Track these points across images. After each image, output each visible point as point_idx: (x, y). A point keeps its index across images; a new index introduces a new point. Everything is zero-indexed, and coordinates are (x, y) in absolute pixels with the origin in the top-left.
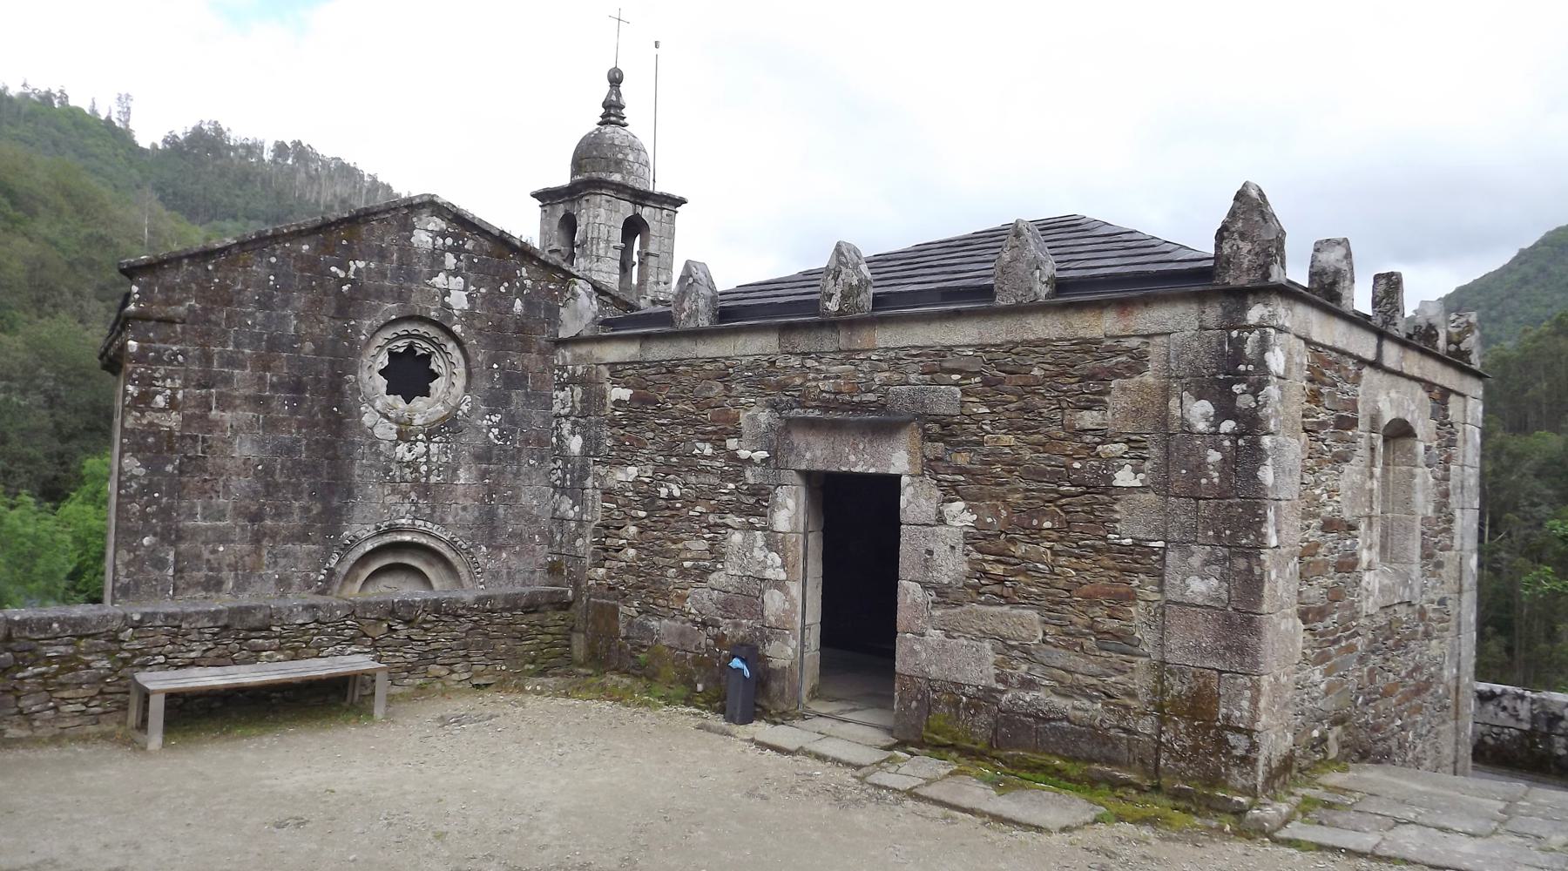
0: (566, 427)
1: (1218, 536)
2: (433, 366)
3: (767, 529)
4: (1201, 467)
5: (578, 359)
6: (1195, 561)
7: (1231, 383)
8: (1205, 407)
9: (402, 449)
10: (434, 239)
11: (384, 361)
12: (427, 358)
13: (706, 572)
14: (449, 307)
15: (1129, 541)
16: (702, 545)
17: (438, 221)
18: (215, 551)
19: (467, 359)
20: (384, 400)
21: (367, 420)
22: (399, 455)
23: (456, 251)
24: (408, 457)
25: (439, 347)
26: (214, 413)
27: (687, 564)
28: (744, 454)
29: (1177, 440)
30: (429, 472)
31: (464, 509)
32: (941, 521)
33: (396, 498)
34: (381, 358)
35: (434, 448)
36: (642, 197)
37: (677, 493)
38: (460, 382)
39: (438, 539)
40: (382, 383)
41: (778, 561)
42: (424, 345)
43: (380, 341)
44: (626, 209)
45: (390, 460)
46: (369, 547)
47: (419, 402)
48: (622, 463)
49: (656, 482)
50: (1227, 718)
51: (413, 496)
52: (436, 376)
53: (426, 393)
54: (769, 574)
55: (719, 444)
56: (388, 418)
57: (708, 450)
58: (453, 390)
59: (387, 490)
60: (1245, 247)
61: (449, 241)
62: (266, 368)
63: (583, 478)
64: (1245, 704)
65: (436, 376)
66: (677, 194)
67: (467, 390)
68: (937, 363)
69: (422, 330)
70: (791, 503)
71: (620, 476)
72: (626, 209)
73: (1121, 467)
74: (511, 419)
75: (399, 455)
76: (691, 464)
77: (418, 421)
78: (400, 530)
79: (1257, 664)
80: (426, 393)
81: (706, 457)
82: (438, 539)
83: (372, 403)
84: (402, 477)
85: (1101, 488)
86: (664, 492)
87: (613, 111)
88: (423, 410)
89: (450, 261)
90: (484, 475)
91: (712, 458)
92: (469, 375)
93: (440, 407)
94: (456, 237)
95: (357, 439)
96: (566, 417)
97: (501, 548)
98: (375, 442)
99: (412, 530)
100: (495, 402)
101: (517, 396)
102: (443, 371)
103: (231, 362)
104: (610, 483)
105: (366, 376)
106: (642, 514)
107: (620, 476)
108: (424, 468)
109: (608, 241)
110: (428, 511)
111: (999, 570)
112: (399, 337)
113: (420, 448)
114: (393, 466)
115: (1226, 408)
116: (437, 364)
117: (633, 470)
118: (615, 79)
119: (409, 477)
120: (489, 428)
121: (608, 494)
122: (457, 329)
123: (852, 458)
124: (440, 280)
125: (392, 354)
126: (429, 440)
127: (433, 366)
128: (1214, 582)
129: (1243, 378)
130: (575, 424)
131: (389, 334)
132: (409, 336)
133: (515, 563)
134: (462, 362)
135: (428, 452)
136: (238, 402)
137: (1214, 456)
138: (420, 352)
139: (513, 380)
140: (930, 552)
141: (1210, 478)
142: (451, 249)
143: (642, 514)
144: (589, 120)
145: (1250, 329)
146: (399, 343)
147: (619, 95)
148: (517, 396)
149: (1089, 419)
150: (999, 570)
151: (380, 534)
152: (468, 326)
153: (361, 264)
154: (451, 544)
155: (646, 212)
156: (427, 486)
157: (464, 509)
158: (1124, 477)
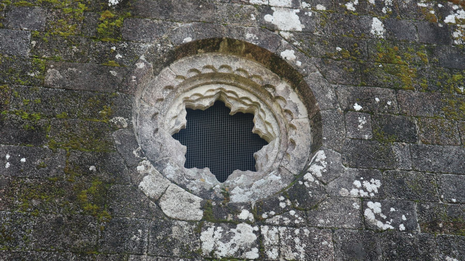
9: (210, 239)
14: (272, 28)
19: (309, 100)
21: (149, 185)
22: (207, 247)
25: (263, 90)
34: (174, 111)
35: (271, 235)
42: (241, 94)
53: (250, 165)
65: (262, 141)
69: (236, 65)
75: (207, 247)
80: (250, 165)
92: (316, 120)
95: (131, 217)
100: (365, 160)
102: (274, 129)
113: (245, 234)
120: (363, 201)
122: (288, 55)
127: (258, 126)
131: (181, 68)
132: (214, 77)
134: (302, 109)
135: (261, 238)
146: (203, 90)
152: (303, 53)
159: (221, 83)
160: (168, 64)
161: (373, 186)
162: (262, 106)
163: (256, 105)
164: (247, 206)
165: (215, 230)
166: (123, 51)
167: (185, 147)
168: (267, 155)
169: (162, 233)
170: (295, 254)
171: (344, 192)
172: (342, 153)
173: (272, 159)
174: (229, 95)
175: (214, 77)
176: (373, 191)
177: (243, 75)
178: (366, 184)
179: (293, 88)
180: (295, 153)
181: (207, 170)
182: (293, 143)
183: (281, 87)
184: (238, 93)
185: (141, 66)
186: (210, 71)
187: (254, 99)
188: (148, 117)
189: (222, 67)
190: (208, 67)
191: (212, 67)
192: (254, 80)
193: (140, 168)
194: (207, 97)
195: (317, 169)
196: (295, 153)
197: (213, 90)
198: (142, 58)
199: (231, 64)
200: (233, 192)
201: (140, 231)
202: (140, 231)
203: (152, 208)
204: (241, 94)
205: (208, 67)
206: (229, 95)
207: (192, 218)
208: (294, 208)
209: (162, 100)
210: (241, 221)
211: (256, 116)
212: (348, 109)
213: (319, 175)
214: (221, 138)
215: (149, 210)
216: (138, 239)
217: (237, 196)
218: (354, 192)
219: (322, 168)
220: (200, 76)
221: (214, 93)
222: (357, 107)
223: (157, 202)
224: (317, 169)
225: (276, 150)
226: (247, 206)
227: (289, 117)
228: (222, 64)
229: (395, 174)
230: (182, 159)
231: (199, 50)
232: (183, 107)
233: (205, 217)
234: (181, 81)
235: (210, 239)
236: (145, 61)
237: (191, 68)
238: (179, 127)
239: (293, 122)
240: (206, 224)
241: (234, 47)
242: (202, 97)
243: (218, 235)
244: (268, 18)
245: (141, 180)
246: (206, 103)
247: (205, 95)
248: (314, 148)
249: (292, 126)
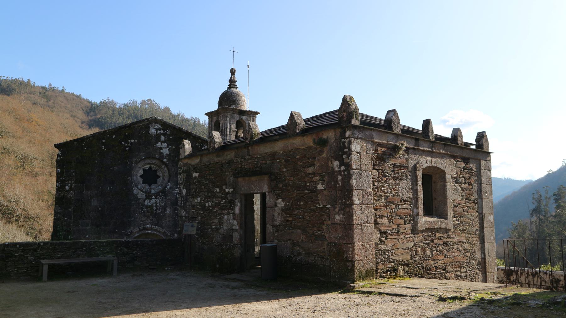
0: (182, 186)
1: (342, 201)
2: (158, 174)
3: (234, 214)
4: (336, 182)
5: (185, 165)
6: (337, 210)
7: (342, 155)
8: (336, 163)
9: (147, 202)
10: (157, 131)
12: (156, 171)
13: (218, 229)
14: (162, 153)
15: (321, 206)
16: (217, 220)
17: (158, 125)
22: (146, 204)
23: (164, 135)
24: (149, 204)
25: (159, 166)
27: (213, 227)
28: (227, 190)
29: (332, 174)
30: (157, 209)
31: (169, 221)
32: (276, 205)
36: (243, 113)
37: (210, 205)
39: (159, 232)
40: (141, 180)
41: (236, 223)
44: (237, 117)
46: (137, 235)
47: (153, 186)
48: (196, 197)
49: (205, 202)
50: (346, 257)
53: (156, 182)
54: (234, 227)
55: (221, 188)
56: (143, 192)
57: (218, 190)
60: (345, 114)
61: (162, 132)
63: (186, 202)
64: (350, 252)
65: (159, 177)
66: (256, 111)
68: (273, 156)
69: (154, 161)
70: (239, 204)
71: (196, 201)
72: (237, 117)
73: (318, 184)
75: (146, 204)
76: (214, 195)
77: (153, 192)
78: (147, 229)
79: (353, 239)
80: (156, 182)
81: (217, 193)
83: (137, 186)
84: (147, 211)
85: (315, 191)
86: (207, 205)
87: (232, 83)
88: (155, 189)
89: (163, 138)
91: (219, 192)
92: (170, 175)
93: (160, 187)
94: (164, 131)
96: (182, 183)
99: (151, 229)
102: (161, 175)
104: (193, 203)
105: (135, 178)
106: (202, 212)
107: (196, 201)
108: (155, 208)
109: (230, 129)
111: (290, 219)
112: (146, 164)
113: (153, 201)
115: (342, 163)
116: (159, 173)
117: (199, 199)
118: (233, 72)
121: (193, 207)
122: (165, 160)
123: (254, 188)
124: (159, 144)
127: (158, 174)
128: (341, 216)
129: (345, 153)
130: (184, 185)
134: (167, 171)
137: (340, 178)
138: (153, 169)
140: (274, 216)
141: (339, 184)
142: (162, 134)
143: (202, 212)
144: (224, 87)
145: (347, 138)
146: (146, 166)
147: (234, 77)
149: (310, 170)
150: (290, 219)
151: (140, 231)
153: (133, 141)
155: (244, 118)
156: (156, 214)
157: (169, 221)
158: (320, 187)
166: (129, 161)
168: (160, 180)
175: (149, 164)
195: (168, 187)
196: (165, 182)
203: (136, 196)
217: (153, 192)
224: (168, 187)
230: (141, 182)
235: (147, 202)
241: (154, 158)
244: (161, 151)
247: (147, 167)
248: (169, 181)
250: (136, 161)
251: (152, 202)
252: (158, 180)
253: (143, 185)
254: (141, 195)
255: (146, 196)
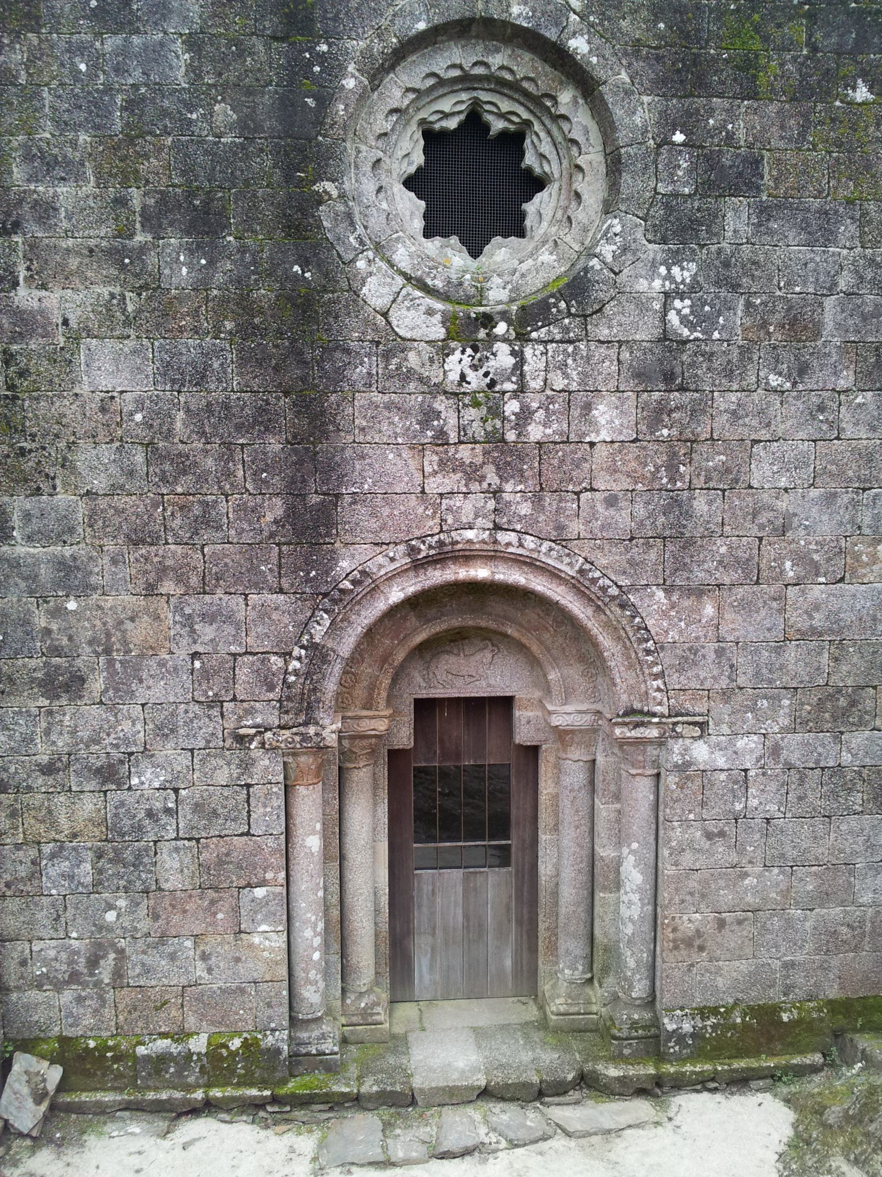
11: (411, 153)
12: (513, 141)
18: (58, 612)
20: (413, 247)
21: (376, 290)
26: (25, 297)
31: (612, 501)
33: (451, 481)
34: (405, 145)
38: (592, 189)
40: (411, 208)
42: (505, 106)
43: (395, 91)
45: (439, 389)
46: (396, 595)
47: (501, 252)
51: (492, 478)
52: (538, 183)
53: (516, 228)
58: (580, 215)
59: (431, 461)
62: (129, 177)
67: (608, 208)
69: (497, 60)
74: (726, 276)
78: (467, 557)
80: (516, 228)
82: (554, 574)
88: (513, 268)
90: (657, 416)
92: (615, 165)
93: (546, 257)
97: (699, 592)
98: (392, 345)
99: (494, 556)
100: (680, 228)
101: (736, 219)
102: (553, 168)
103: (48, 165)
105: (369, 186)
108: (512, 407)
110: (525, 509)
113: (502, 358)
114: (441, 404)
119: (477, 430)
125: (433, 138)
126: (523, 338)
127: (530, 159)
131: (413, 74)
132: (466, 81)
133: (735, 625)
136: (74, 263)
138: (498, 125)
139: (726, 175)
146: (446, 105)
148: (736, 219)
151: (418, 565)
154: (579, 586)
157: (612, 501)
159: (475, 89)
160: (392, 68)
161: (683, 274)
162: (537, 127)
163: (528, 123)
164: (505, 316)
165: (463, 352)
167: (423, 204)
169: (395, 361)
170: (566, 381)
171: (642, 285)
172: (645, 221)
173: (547, 218)
174: (487, 107)
176: (683, 282)
177: (508, 77)
178: (676, 270)
179: (585, 97)
180: (580, 215)
181: (454, 240)
182: (578, 196)
183: (566, 97)
184: (500, 104)
185: (350, 83)
186: (457, 73)
187: (525, 115)
188: (367, 168)
189: (475, 64)
190: (453, 66)
191: (460, 67)
192: (525, 85)
193: (361, 264)
194: (453, 114)
195: (607, 250)
197: (463, 102)
198: (351, 68)
199: (490, 60)
200: (489, 285)
201: (366, 359)
202: (366, 359)
204: (505, 106)
205: (453, 66)
206: (487, 107)
207: (432, 337)
208: (570, 315)
209: (385, 134)
210: (495, 338)
211: (528, 141)
212: (666, 142)
213: (609, 259)
214: (476, 182)
215: (376, 329)
216: (365, 371)
218: (657, 284)
219: (614, 248)
220: (441, 82)
221: (463, 107)
222: (679, 137)
223: (385, 315)
225: (553, 204)
226: (505, 316)
227: (574, 151)
228: (475, 59)
229: (719, 251)
230: (418, 224)
231: (440, 38)
232: (419, 135)
233: (449, 337)
234: (412, 96)
236: (357, 74)
237: (428, 71)
238: (412, 169)
239: (580, 161)
240: (453, 344)
242: (446, 116)
243: (467, 360)
245: (363, 284)
246: (452, 124)
249: (579, 168)
250: (367, 54)
251: (492, 365)
252: (530, 208)
253: (433, 246)
254: (418, 321)
255: (447, 320)
